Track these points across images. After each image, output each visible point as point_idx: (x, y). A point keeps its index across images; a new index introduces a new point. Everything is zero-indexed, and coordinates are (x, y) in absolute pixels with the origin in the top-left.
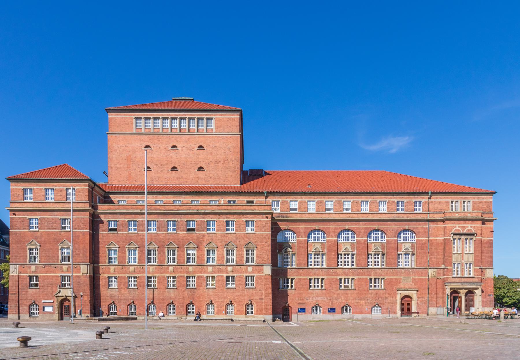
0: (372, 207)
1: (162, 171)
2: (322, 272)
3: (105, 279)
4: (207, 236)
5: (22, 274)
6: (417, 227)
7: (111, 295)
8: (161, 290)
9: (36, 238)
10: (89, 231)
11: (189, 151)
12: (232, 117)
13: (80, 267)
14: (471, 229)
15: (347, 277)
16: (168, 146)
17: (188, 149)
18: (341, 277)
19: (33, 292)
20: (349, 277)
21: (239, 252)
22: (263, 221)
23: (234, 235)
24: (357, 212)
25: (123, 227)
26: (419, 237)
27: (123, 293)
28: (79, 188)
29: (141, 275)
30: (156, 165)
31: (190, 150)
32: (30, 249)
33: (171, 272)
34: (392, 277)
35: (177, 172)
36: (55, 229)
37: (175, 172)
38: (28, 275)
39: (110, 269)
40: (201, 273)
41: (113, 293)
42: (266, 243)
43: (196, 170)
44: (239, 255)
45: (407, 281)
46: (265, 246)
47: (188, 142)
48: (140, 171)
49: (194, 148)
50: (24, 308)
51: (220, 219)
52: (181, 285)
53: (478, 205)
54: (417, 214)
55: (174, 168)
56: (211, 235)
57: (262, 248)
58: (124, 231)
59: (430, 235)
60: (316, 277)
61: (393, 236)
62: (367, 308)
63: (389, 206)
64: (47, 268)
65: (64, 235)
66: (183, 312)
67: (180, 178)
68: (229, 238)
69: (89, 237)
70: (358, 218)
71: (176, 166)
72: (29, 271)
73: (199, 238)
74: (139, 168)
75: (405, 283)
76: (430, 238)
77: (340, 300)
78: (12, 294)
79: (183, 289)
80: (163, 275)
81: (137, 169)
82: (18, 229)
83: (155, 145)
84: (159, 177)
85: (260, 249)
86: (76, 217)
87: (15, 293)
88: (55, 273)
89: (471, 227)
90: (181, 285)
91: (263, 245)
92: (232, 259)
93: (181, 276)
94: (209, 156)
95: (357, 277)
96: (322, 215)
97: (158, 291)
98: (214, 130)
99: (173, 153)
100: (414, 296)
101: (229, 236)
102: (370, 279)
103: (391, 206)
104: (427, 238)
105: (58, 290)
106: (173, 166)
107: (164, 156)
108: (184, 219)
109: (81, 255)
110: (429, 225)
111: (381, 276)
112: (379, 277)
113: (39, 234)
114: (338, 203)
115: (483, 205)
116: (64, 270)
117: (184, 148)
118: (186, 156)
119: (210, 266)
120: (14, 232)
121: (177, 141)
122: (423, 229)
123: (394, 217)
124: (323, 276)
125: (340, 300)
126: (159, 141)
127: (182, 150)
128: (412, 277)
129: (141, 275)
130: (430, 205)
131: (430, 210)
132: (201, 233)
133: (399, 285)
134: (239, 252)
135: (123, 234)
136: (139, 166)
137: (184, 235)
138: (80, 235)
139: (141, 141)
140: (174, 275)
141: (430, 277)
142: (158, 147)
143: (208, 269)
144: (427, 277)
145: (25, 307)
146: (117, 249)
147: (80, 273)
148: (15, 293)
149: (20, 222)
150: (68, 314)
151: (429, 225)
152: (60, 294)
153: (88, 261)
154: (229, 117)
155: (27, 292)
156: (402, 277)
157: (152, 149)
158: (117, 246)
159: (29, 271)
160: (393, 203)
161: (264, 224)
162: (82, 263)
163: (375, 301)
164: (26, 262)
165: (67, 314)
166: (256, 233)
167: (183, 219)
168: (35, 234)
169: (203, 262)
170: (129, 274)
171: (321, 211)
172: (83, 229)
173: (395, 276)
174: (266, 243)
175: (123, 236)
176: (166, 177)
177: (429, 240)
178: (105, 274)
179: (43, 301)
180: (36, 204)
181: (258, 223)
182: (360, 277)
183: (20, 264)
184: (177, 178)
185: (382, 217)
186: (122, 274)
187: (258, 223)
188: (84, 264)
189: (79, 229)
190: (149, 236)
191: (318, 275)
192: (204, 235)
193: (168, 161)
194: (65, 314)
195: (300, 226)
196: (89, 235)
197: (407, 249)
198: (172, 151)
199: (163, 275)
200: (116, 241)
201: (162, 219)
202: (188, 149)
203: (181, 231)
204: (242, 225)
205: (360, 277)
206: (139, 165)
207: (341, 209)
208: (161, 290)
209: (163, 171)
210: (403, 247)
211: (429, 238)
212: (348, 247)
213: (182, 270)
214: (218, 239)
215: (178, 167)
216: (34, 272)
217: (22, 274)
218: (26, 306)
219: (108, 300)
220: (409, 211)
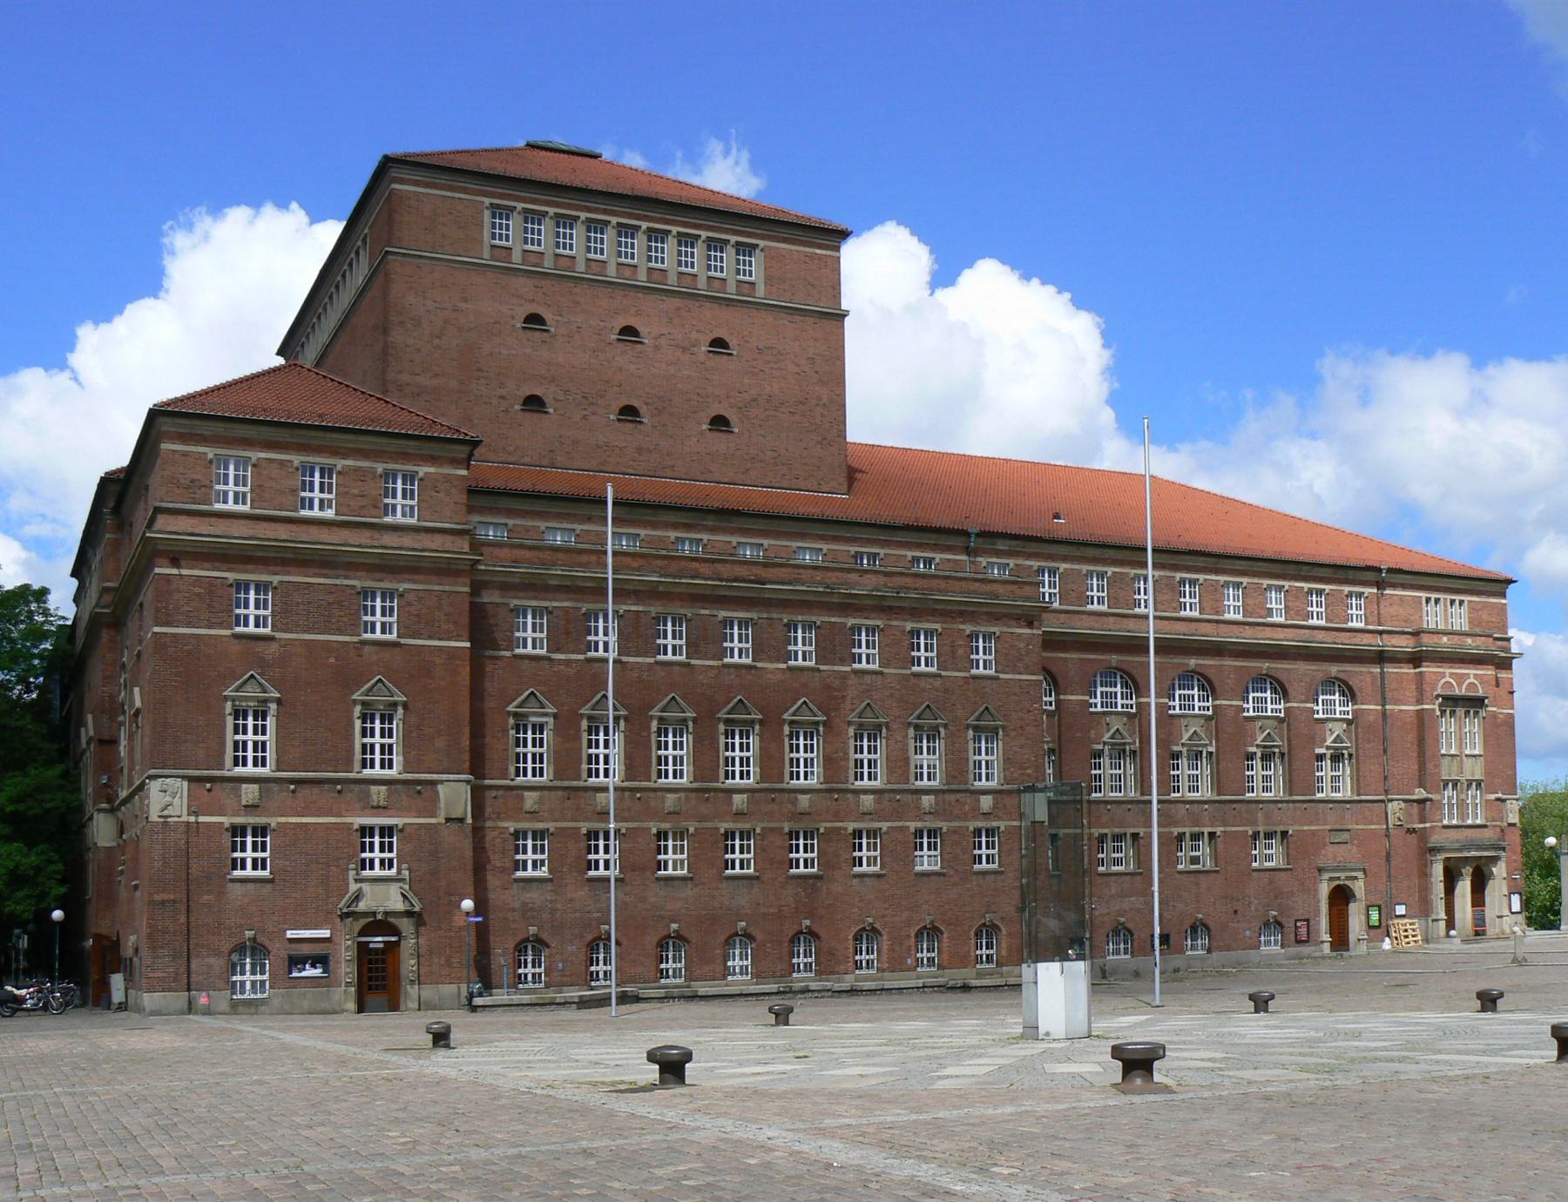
0: (1250, 602)
1: (585, 417)
2: (1131, 813)
3: (504, 840)
4: (853, 680)
5: (202, 819)
6: (1356, 672)
7: (525, 904)
8: (704, 884)
9: (263, 665)
10: (468, 645)
11: (679, 353)
12: (818, 251)
13: (437, 792)
14: (1476, 682)
15: (1196, 829)
16: (608, 325)
17: (677, 346)
18: (1181, 830)
19: (245, 895)
20: (1202, 829)
21: (953, 743)
22: (1020, 635)
23: (938, 683)
24: (1216, 617)
25: (568, 633)
26: (1362, 704)
27: (569, 896)
28: (432, 470)
29: (635, 825)
30: (566, 392)
31: (684, 349)
32: (239, 713)
33: (739, 814)
34: (1306, 828)
35: (639, 427)
36: (340, 632)
37: (631, 425)
38: (226, 821)
39: (522, 798)
40: (838, 817)
41: (534, 896)
42: (1029, 711)
43: (705, 427)
44: (953, 754)
45: (1340, 840)
46: (1028, 725)
47: (675, 321)
48: (506, 411)
49: (696, 344)
50: (210, 966)
51: (895, 623)
52: (771, 865)
53: (1480, 613)
54: (1355, 634)
55: (629, 412)
56: (867, 678)
57: (1020, 731)
58: (573, 652)
59: (1388, 695)
60: (1117, 830)
61: (1303, 697)
62: (1250, 929)
63: (1290, 604)
64: (306, 792)
65: (374, 658)
66: (779, 967)
67: (649, 451)
68: (924, 690)
69: (468, 668)
70: (1218, 636)
71: (635, 403)
72: (230, 802)
73: (828, 687)
74: (502, 397)
75: (1336, 846)
76: (1387, 707)
77: (1180, 906)
78: (163, 903)
79: (780, 879)
80: (710, 825)
81: (494, 401)
82: (188, 625)
83: (561, 315)
84: (576, 442)
85: (1013, 734)
86: (421, 587)
87: (174, 901)
88: (339, 815)
89: (1451, 675)
90: (771, 865)
91: (1021, 719)
92: (929, 767)
93: (772, 830)
94: (746, 381)
95: (1222, 829)
96: (1125, 621)
97: (696, 885)
98: (761, 290)
99: (623, 357)
100: (1359, 888)
101: (922, 683)
102: (1255, 836)
103: (1297, 604)
104: (1380, 707)
105: (353, 887)
106: (625, 402)
107: (592, 361)
108: (779, 616)
109: (440, 743)
110: (1382, 669)
111: (1279, 825)
112: (1275, 828)
113: (274, 647)
114: (1167, 585)
115: (1489, 615)
116: (375, 804)
117: (663, 341)
118: (672, 370)
119: (866, 791)
120: (174, 635)
121: (638, 313)
122: (1369, 680)
123: (1304, 638)
124: (1135, 827)
125: (1180, 906)
126: (578, 303)
127: (657, 348)
128: (1350, 827)
129: (635, 825)
130: (1382, 606)
131: (1382, 620)
132: (836, 668)
133: (1323, 852)
134: (953, 743)
135: (568, 662)
136: (503, 392)
137: (780, 676)
138: (438, 661)
139: (513, 295)
140: (747, 826)
141: (1391, 826)
142: (574, 327)
143: (858, 804)
144: (1385, 827)
145: (212, 960)
146: (551, 720)
147: (433, 816)
148: (172, 897)
149: (198, 595)
150: (384, 987)
151: (1382, 669)
152: (362, 906)
153: (467, 765)
154: (808, 250)
155: (221, 893)
156: (1329, 827)
157: (552, 329)
158: (551, 710)
159: (230, 802)
160: (1300, 595)
161: (1022, 645)
162: (445, 777)
163: (1269, 906)
164: (221, 766)
165: (377, 988)
166: (1002, 676)
167: (775, 616)
168: (260, 647)
169: (843, 778)
170: (587, 819)
171: (1122, 608)
172: (448, 639)
173: (1311, 823)
174: (1029, 711)
175: (571, 671)
176: (601, 443)
177: (1384, 713)
178: (503, 820)
179: (290, 934)
180: (265, 525)
181: (1007, 642)
182: (1228, 829)
183: (197, 773)
184: (639, 450)
185: (1276, 637)
186: (565, 820)
187: (1007, 642)
188: (452, 777)
189: (430, 638)
190: (663, 674)
191: (1121, 824)
192: (843, 677)
193: (608, 382)
194: (370, 988)
195: (1068, 655)
196: (467, 663)
197: (1338, 739)
198: (621, 345)
199: (710, 825)
200: (543, 688)
201: (707, 612)
202: (677, 346)
203: (771, 660)
204: (960, 645)
205: (1228, 829)
206: (502, 386)
207: (1175, 605)
208: (704, 884)
209: (593, 418)
210: (1328, 733)
211: (1383, 705)
212: (1198, 730)
213: (775, 807)
214: (888, 693)
215: (643, 410)
216: (252, 808)
217: (202, 819)
218: (217, 953)
219: (513, 926)
220: (1337, 620)
